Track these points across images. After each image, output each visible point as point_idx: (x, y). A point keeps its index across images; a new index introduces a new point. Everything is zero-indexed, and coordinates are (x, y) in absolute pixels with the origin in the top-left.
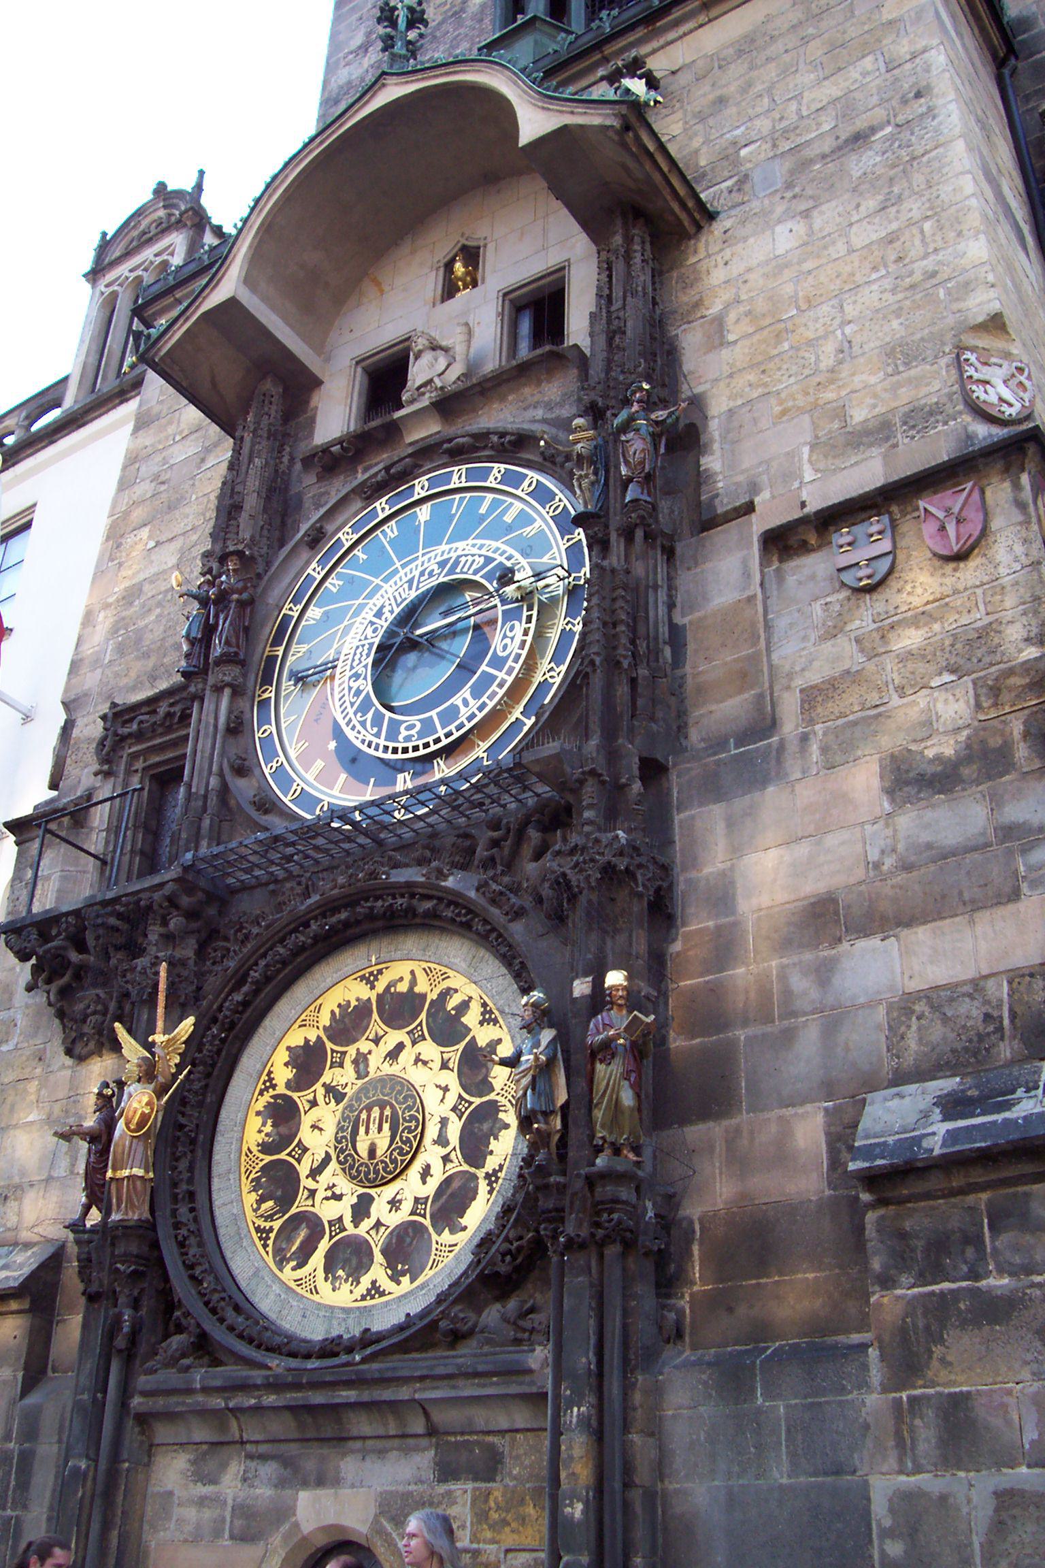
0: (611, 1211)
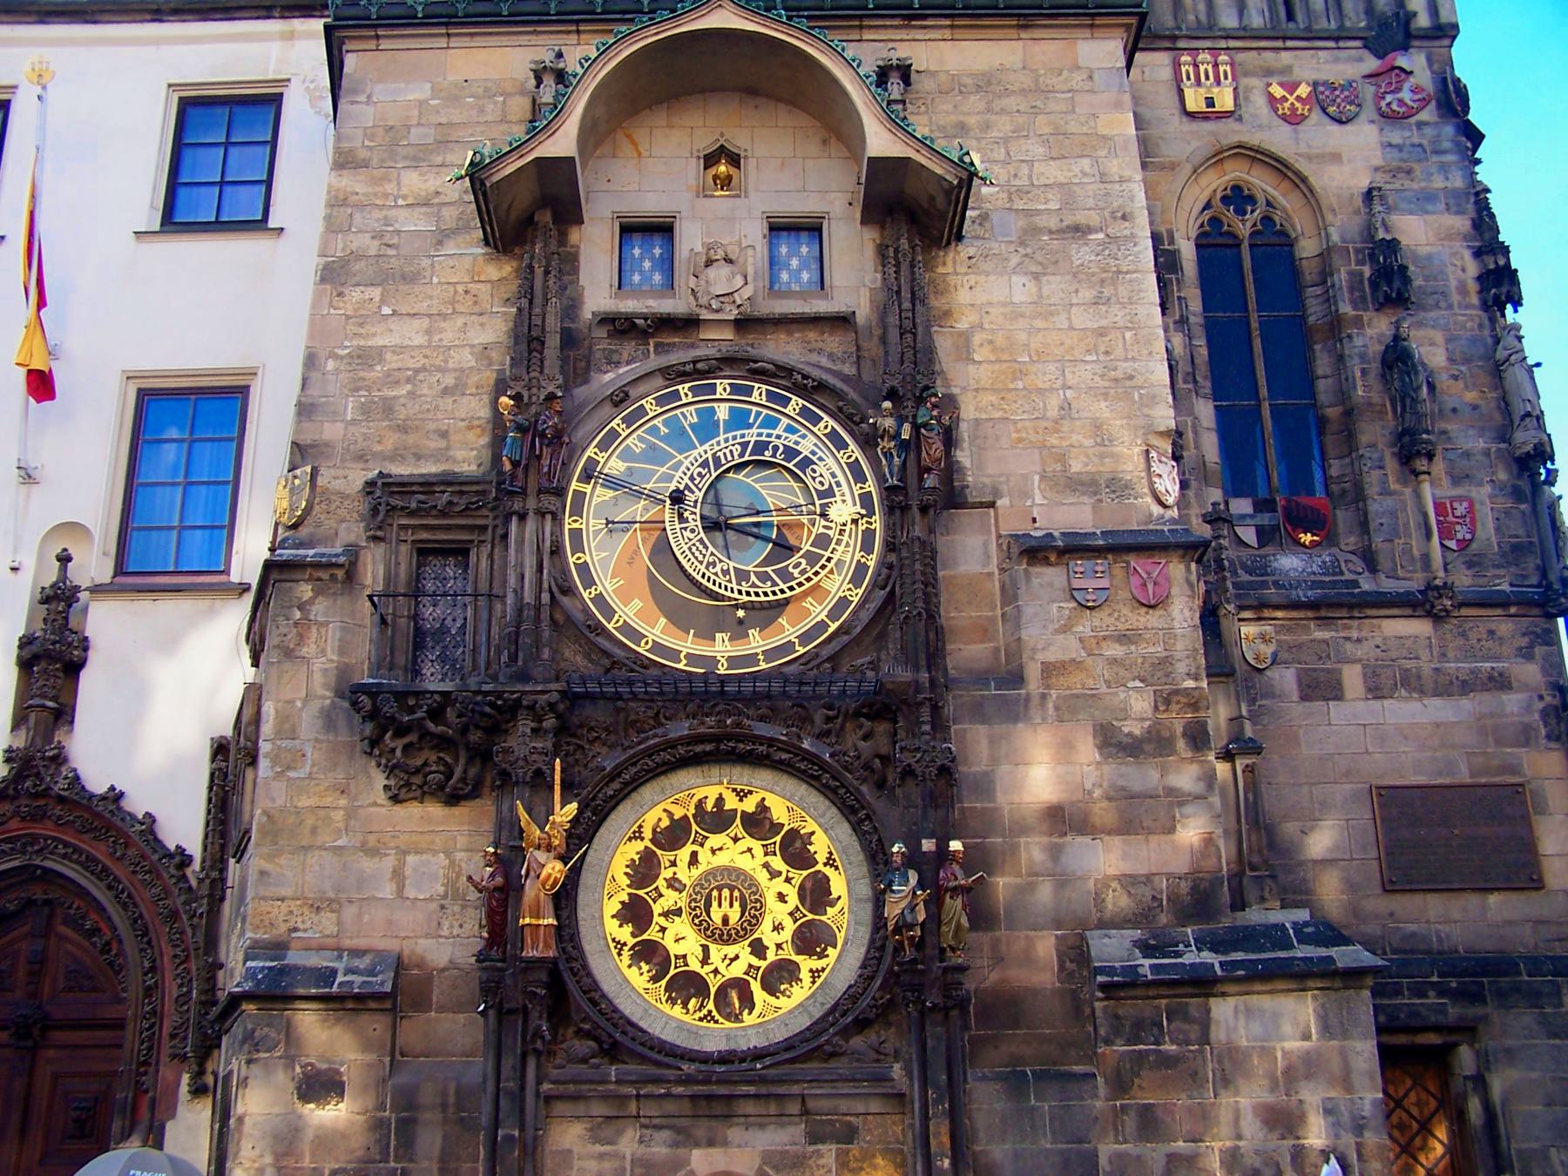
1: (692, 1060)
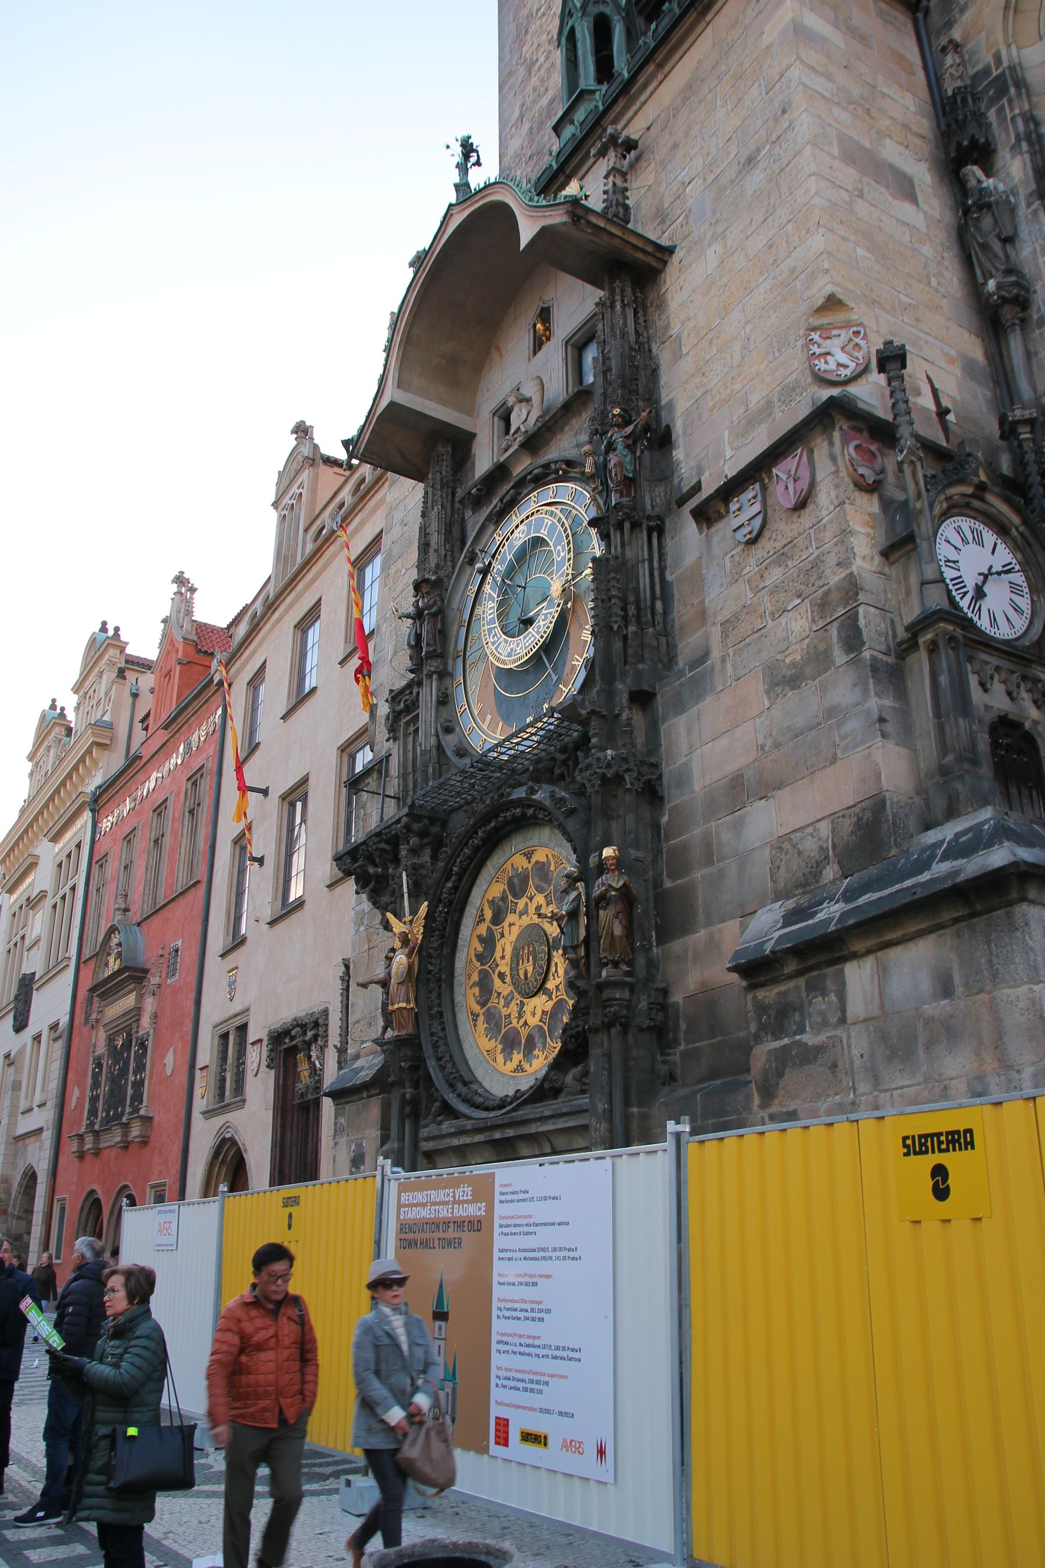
0: (611, 1006)
1: (487, 1109)
